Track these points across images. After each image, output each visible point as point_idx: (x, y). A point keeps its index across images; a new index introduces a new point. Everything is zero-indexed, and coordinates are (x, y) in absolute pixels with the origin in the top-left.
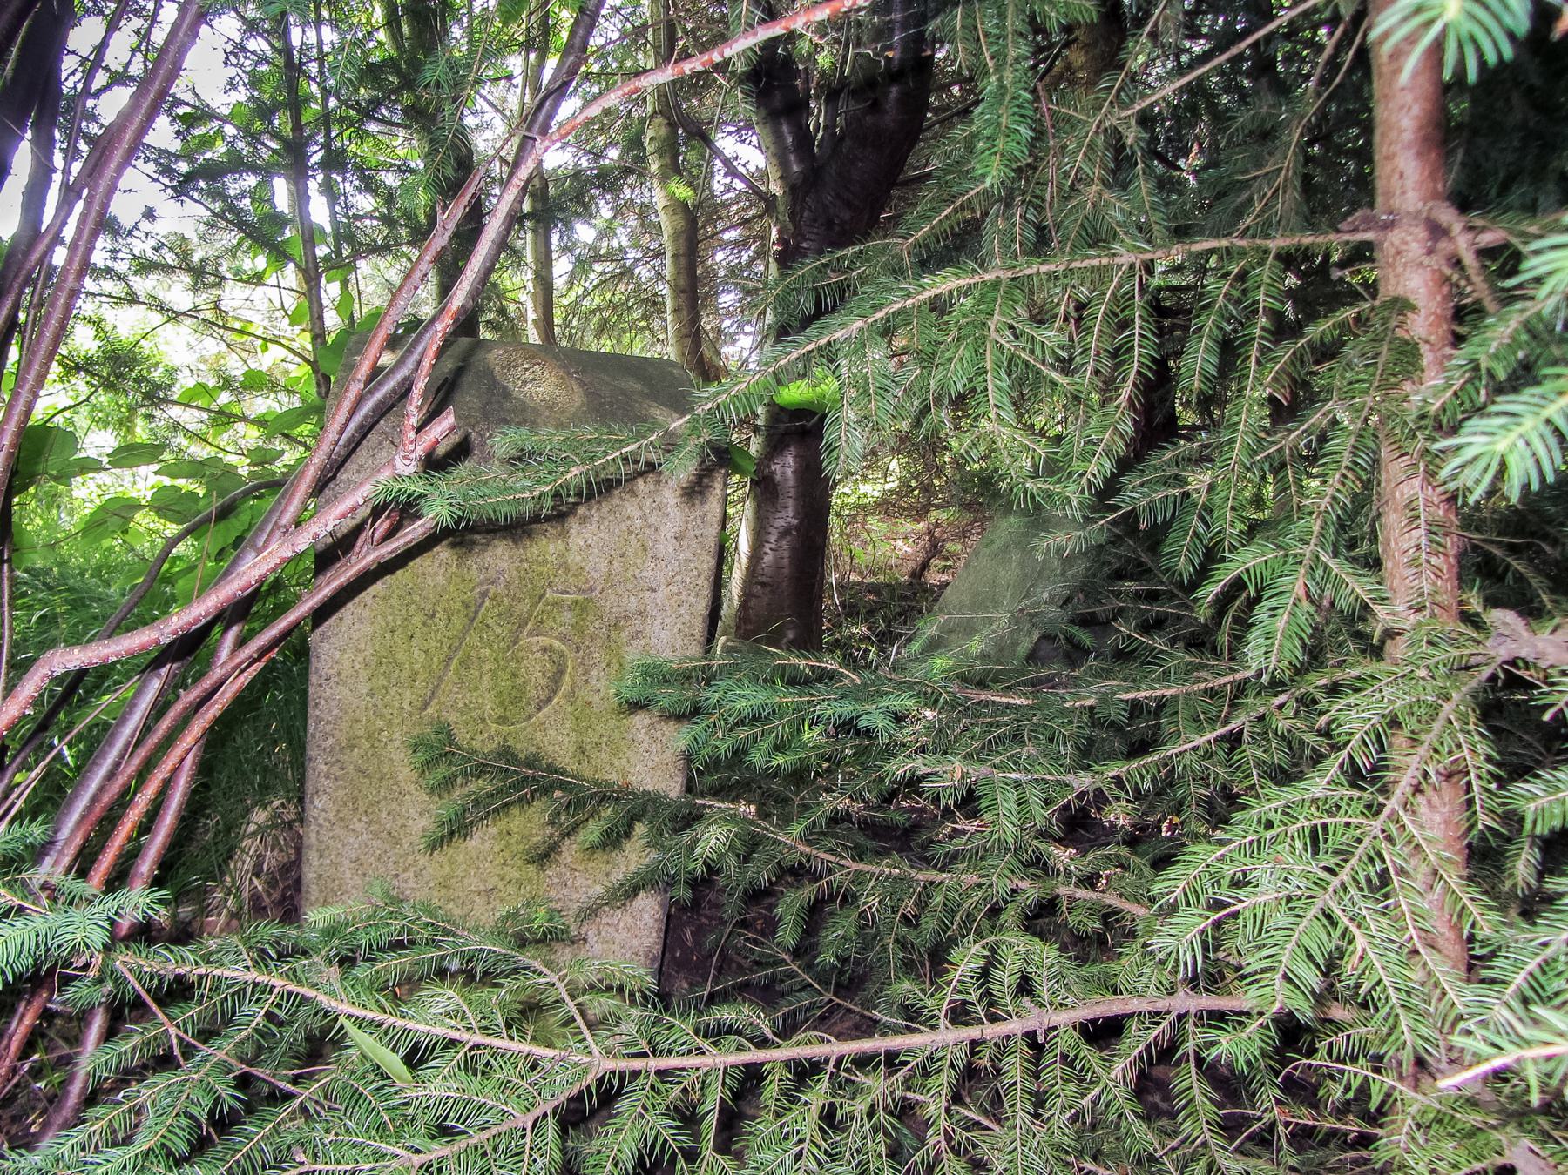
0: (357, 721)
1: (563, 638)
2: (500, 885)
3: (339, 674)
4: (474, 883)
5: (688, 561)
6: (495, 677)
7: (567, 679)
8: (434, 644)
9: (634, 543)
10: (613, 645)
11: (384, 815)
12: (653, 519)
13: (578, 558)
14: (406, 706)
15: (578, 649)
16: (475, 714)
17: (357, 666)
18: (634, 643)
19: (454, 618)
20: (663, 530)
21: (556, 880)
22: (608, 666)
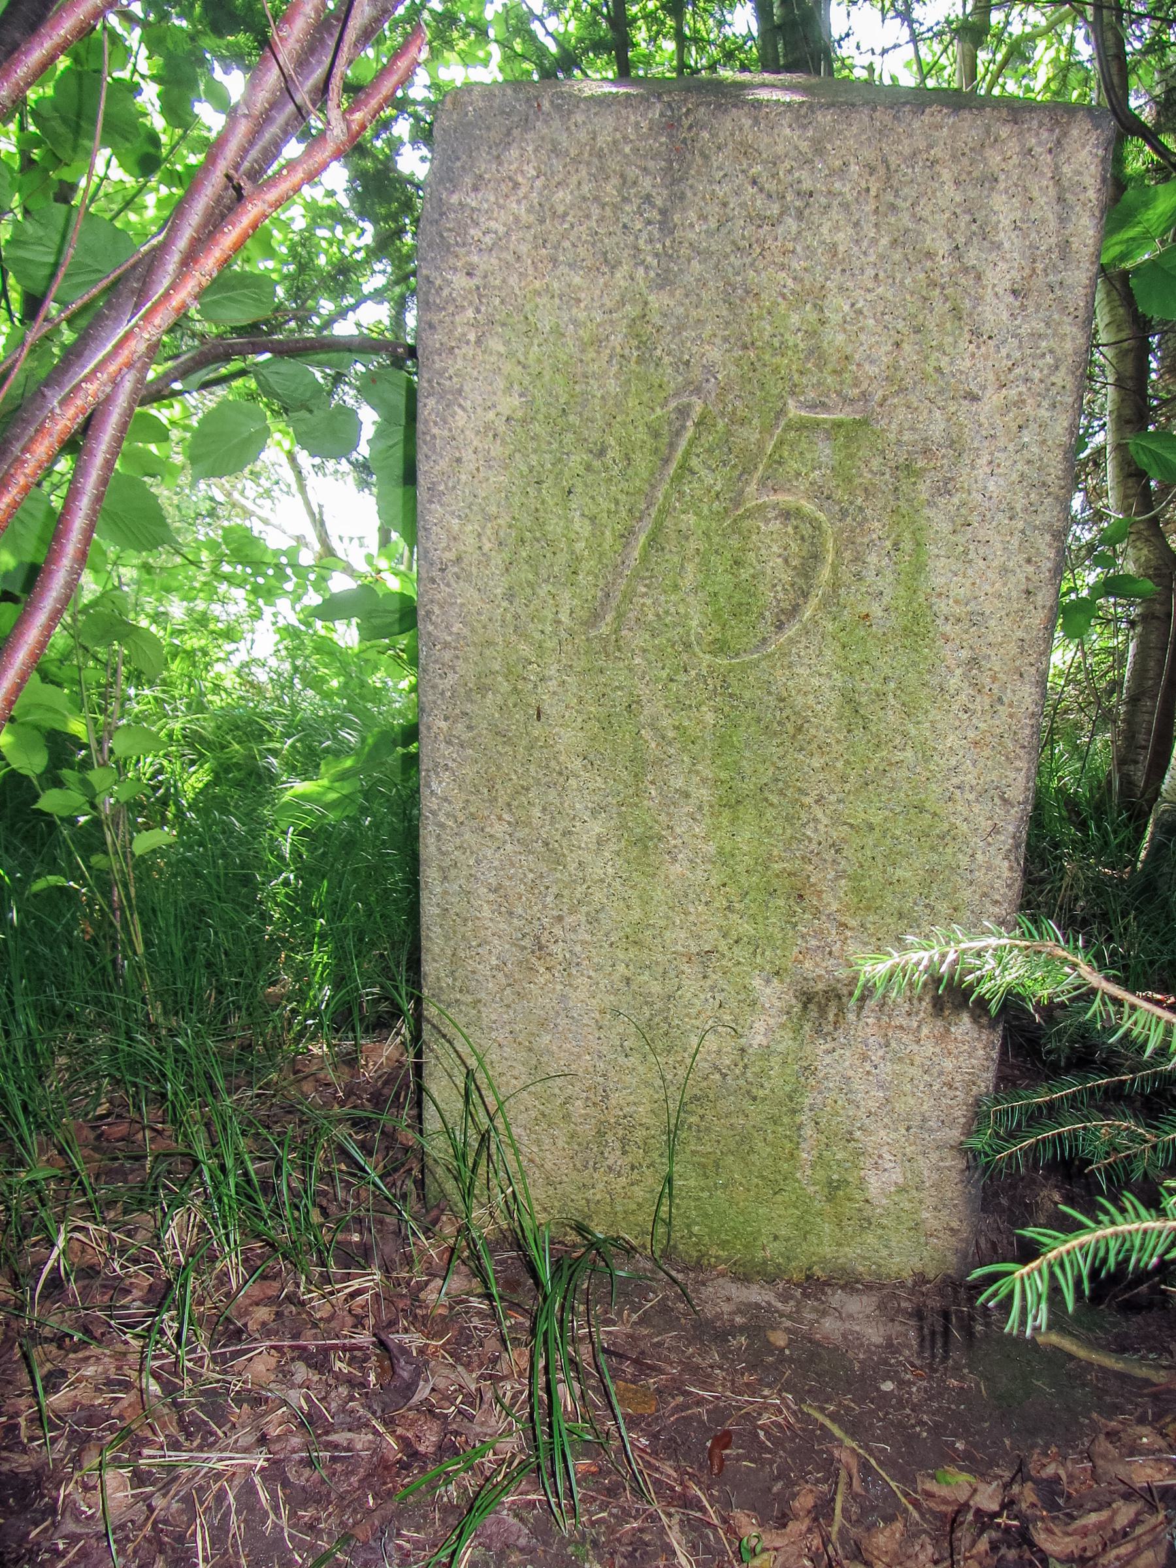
0: (489, 643)
1: (822, 495)
2: (723, 946)
3: (459, 560)
4: (678, 938)
5: (1037, 336)
6: (706, 568)
7: (825, 573)
8: (605, 505)
9: (941, 307)
10: (904, 507)
11: (536, 812)
12: (972, 256)
13: (841, 338)
14: (564, 617)
15: (844, 513)
16: (674, 634)
17: (487, 546)
18: (941, 501)
19: (637, 457)
20: (991, 277)
21: (814, 943)
22: (896, 546)
